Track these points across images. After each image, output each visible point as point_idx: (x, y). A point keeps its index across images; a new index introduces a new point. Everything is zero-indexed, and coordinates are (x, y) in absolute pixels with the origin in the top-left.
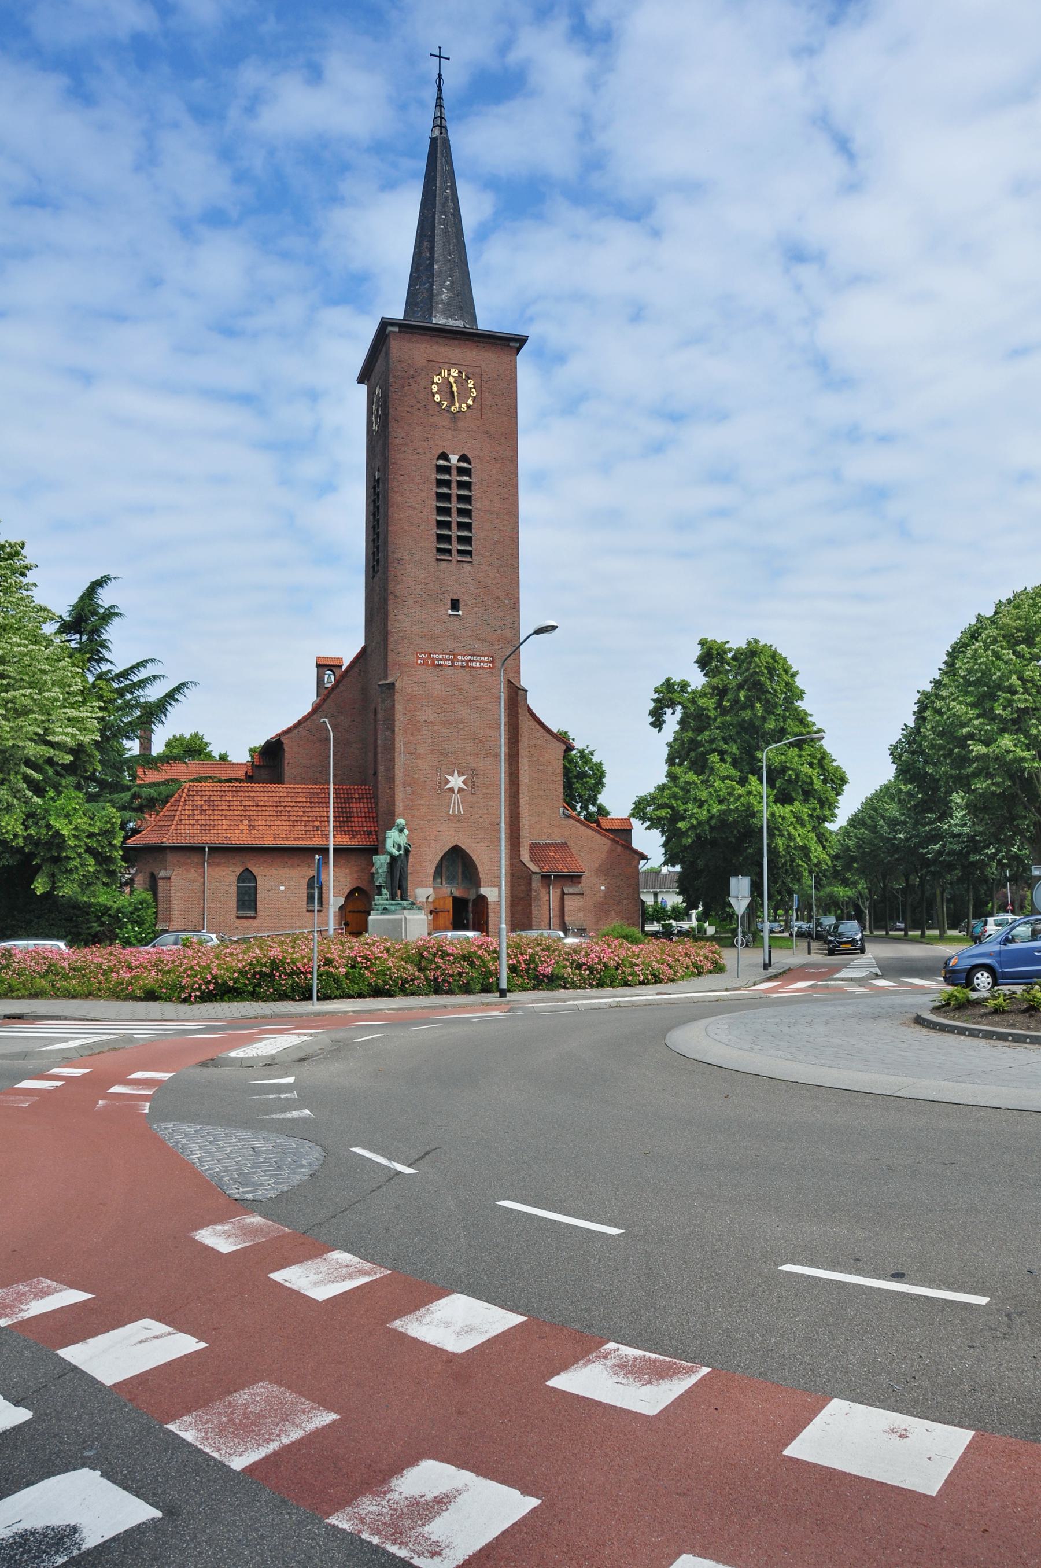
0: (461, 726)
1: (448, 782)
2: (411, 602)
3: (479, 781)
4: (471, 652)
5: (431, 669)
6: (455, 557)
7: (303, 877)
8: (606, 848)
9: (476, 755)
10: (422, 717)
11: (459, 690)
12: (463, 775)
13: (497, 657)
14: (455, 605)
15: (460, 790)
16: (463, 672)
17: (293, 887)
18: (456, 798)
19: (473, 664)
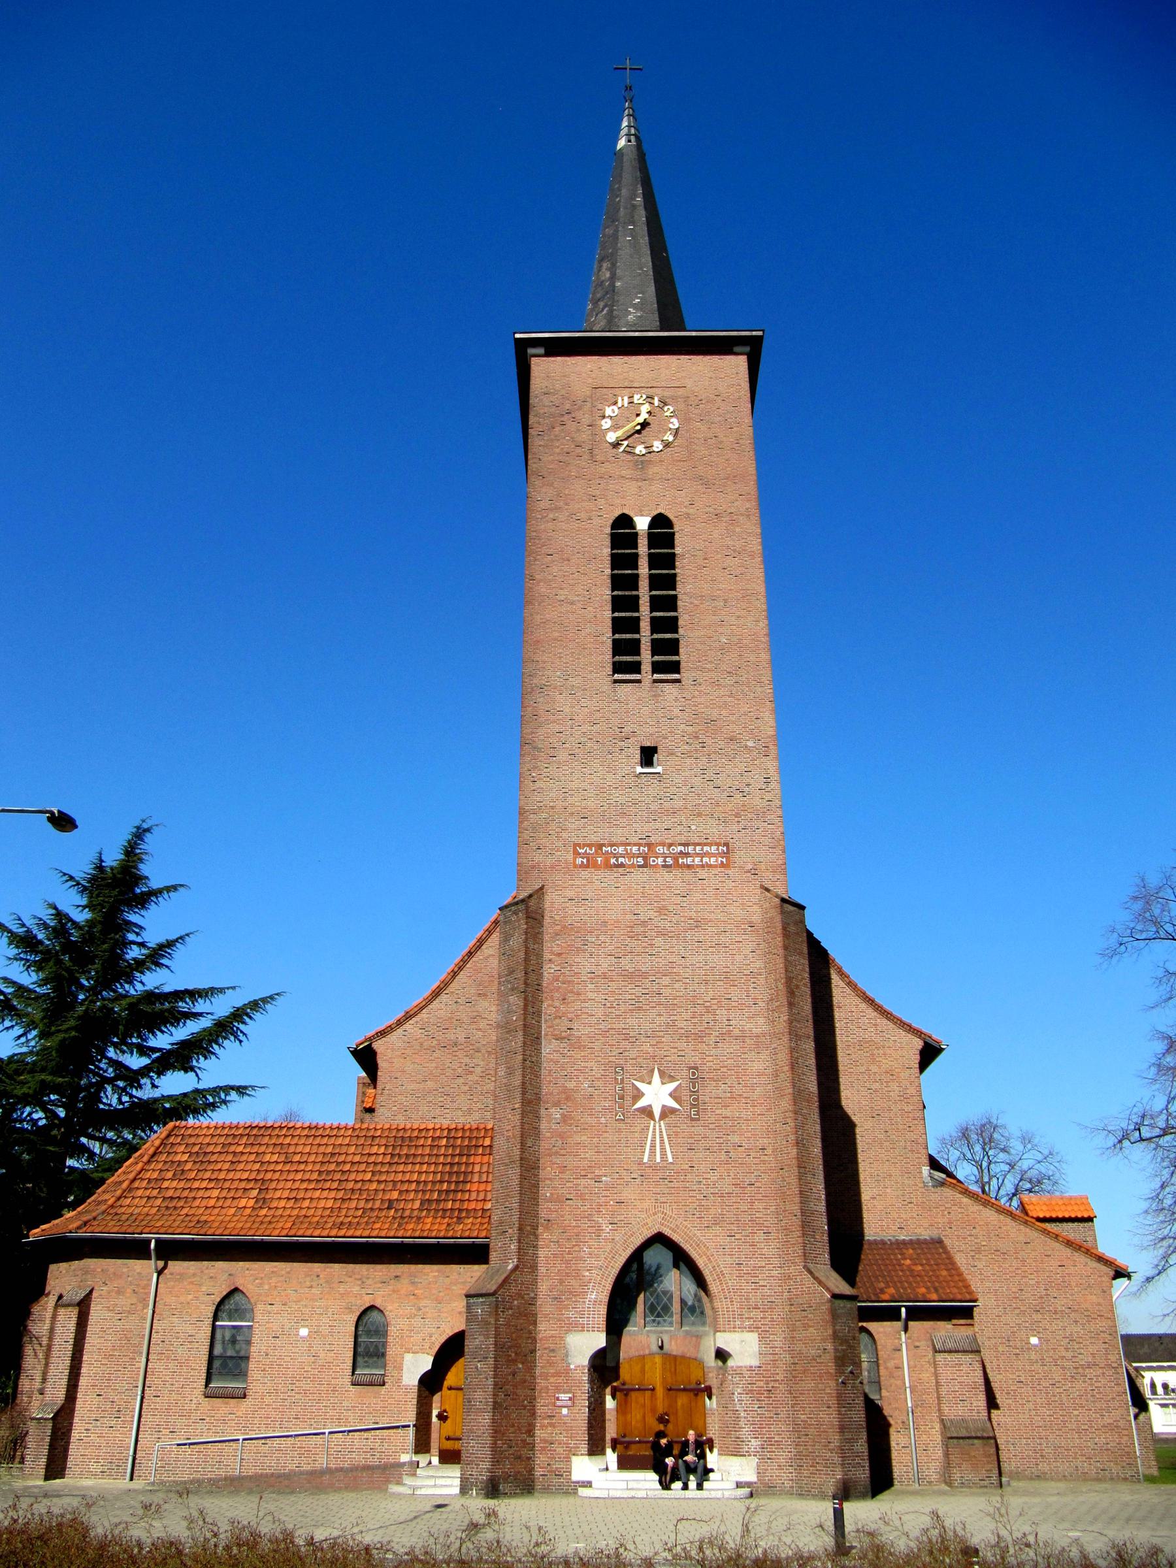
0: (666, 980)
1: (639, 1095)
2: (563, 756)
3: (709, 1092)
4: (683, 840)
5: (610, 876)
7: (349, 1309)
10: (584, 964)
11: (662, 910)
12: (672, 1079)
14: (648, 755)
15: (666, 1112)
16: (666, 876)
17: (325, 1330)
18: (657, 1129)
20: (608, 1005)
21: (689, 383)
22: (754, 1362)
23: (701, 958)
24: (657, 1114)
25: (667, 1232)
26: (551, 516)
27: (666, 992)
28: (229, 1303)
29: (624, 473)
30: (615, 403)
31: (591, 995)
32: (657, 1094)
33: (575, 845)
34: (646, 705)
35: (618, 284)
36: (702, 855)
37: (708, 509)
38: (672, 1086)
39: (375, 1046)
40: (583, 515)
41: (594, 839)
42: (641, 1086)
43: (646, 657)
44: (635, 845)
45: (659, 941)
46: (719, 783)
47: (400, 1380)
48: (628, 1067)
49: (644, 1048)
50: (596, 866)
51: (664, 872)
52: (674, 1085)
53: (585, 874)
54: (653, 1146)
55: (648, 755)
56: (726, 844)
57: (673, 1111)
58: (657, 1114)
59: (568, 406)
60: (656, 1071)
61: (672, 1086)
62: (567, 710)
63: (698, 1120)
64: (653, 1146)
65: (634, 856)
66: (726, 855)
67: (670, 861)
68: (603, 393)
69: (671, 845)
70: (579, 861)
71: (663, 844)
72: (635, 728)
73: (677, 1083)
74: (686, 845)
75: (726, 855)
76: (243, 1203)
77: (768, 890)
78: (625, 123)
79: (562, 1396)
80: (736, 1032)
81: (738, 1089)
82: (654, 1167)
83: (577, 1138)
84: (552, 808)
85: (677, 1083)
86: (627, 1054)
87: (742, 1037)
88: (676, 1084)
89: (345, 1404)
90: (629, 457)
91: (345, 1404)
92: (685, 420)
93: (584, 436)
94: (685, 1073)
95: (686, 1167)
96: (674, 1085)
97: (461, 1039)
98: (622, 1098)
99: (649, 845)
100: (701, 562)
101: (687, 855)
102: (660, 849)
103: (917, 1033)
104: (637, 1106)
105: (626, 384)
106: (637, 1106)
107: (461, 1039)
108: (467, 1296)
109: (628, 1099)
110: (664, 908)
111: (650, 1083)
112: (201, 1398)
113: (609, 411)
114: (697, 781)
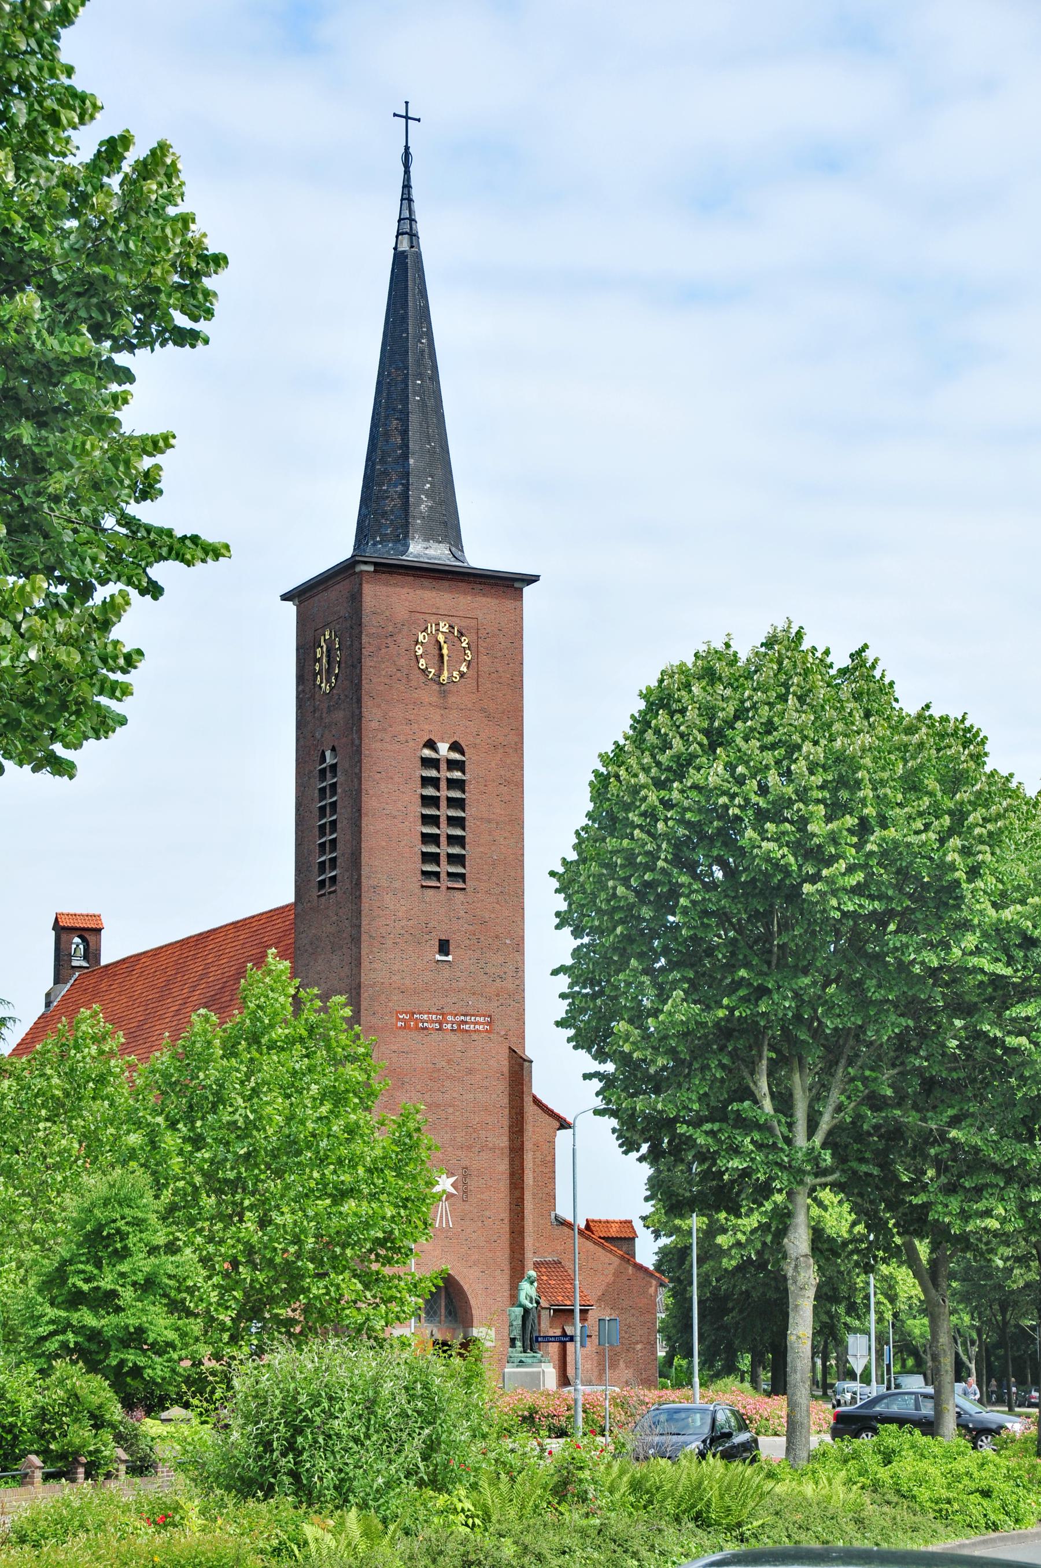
0: (451, 1110)
2: (389, 943)
3: (473, 1184)
4: (464, 1011)
6: (445, 882)
8: (611, 1270)
9: (470, 1148)
11: (449, 1062)
12: (453, 1175)
13: (495, 1017)
16: (453, 1037)
18: (444, 1206)
19: (467, 1027)
21: (480, 617)
27: (451, 1117)
35: (411, 461)
40: (402, 738)
45: (447, 1083)
51: (452, 1035)
53: (402, 1033)
57: (453, 1195)
59: (391, 629)
65: (433, 1022)
66: (489, 1023)
67: (455, 1027)
68: (418, 619)
70: (399, 1024)
71: (451, 1014)
74: (465, 1015)
75: (489, 1023)
81: (490, 1183)
82: (441, 1229)
87: (493, 1149)
92: (477, 654)
93: (402, 662)
99: (443, 1014)
100: (482, 788)
101: (466, 1023)
102: (450, 1018)
113: (421, 638)
114: (473, 968)
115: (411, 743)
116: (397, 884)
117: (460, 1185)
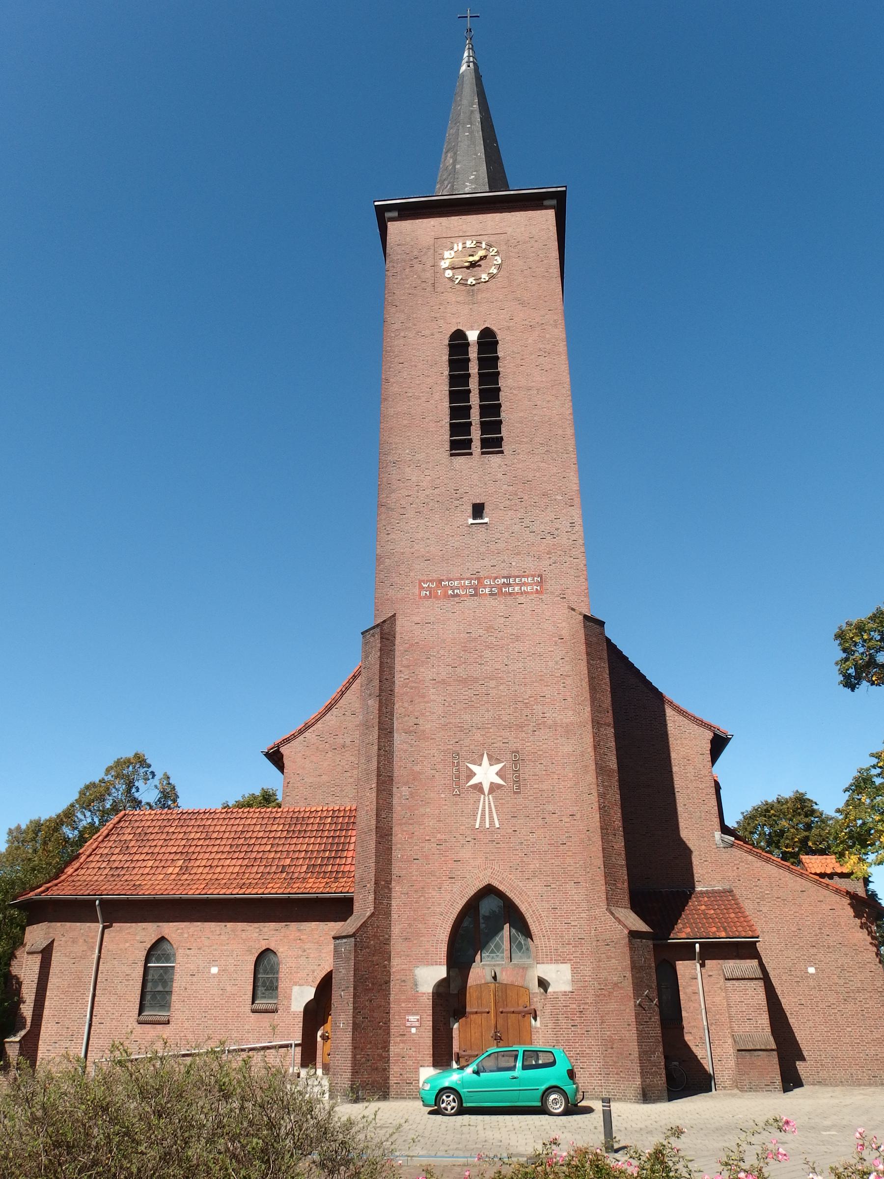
0: (493, 684)
1: (471, 774)
2: (410, 513)
3: (527, 771)
4: (506, 573)
7: (249, 951)
9: (521, 727)
10: (427, 673)
11: (487, 629)
12: (498, 761)
14: (478, 510)
15: (494, 787)
17: (231, 968)
18: (486, 801)
20: (447, 704)
21: (509, 230)
22: (568, 988)
23: (521, 665)
24: (486, 790)
25: (495, 883)
26: (402, 334)
27: (493, 692)
28: (157, 949)
29: (459, 299)
30: (452, 249)
31: (432, 697)
32: (486, 773)
33: (420, 582)
34: (477, 471)
35: (458, 166)
36: (521, 585)
37: (525, 322)
38: (498, 767)
39: (282, 750)
41: (435, 576)
42: (473, 767)
43: (476, 434)
44: (467, 579)
45: (488, 653)
46: (535, 529)
47: (289, 1007)
48: (463, 753)
49: (475, 737)
50: (437, 597)
51: (490, 599)
52: (500, 766)
54: (483, 815)
55: (478, 510)
56: (540, 576)
57: (499, 786)
58: (486, 790)
59: (415, 253)
60: (485, 755)
61: (498, 767)
62: (414, 479)
63: (520, 793)
64: (483, 815)
66: (540, 583)
68: (441, 242)
69: (496, 578)
70: (423, 593)
72: (467, 489)
73: (502, 764)
75: (540, 583)
76: (170, 870)
77: (573, 610)
78: (466, 54)
79: (412, 1018)
80: (550, 722)
82: (482, 830)
83: (422, 810)
84: (403, 553)
85: (502, 764)
86: (462, 742)
87: (554, 726)
88: (502, 765)
89: (246, 1027)
90: (463, 288)
91: (246, 1027)
93: (428, 275)
94: (509, 756)
95: (511, 831)
96: (500, 766)
97: (348, 742)
98: (458, 777)
99: (478, 579)
100: (519, 362)
102: (487, 582)
103: (708, 727)
104: (469, 784)
105: (461, 234)
106: (469, 784)
107: (348, 742)
108: (334, 938)
109: (463, 777)
110: (491, 627)
111: (480, 765)
112: (135, 1024)
114: (516, 528)
115: (437, 336)
116: (421, 456)
117: (510, 775)
